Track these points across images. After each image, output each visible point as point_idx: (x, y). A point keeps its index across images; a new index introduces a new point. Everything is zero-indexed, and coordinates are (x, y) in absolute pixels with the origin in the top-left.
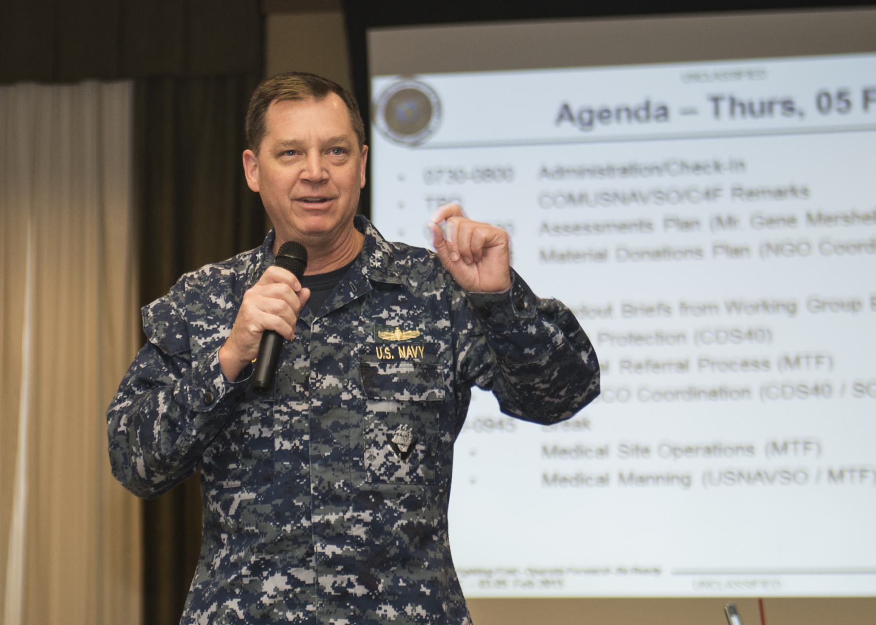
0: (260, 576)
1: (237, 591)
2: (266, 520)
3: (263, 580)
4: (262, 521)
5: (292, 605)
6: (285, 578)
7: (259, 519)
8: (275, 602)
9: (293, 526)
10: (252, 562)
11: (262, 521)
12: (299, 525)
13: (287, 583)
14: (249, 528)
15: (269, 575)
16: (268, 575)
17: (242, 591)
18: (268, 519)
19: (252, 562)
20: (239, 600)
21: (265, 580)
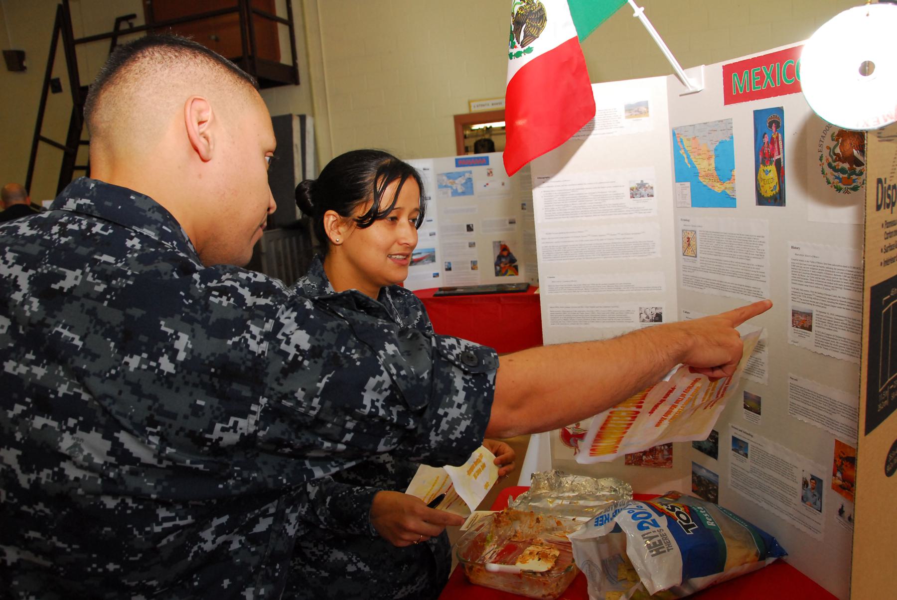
0: (63, 422)
1: (19, 436)
2: (105, 336)
3: (64, 431)
4: (100, 333)
5: (112, 487)
6: (107, 445)
7: (94, 327)
8: (85, 476)
9: (142, 361)
10: (60, 395)
11: (100, 333)
12: (153, 364)
13: (109, 454)
14: (66, 333)
15: (78, 427)
16: (75, 425)
17: (26, 438)
18: (110, 333)
19: (60, 395)
20: (19, 453)
21: (68, 433)
